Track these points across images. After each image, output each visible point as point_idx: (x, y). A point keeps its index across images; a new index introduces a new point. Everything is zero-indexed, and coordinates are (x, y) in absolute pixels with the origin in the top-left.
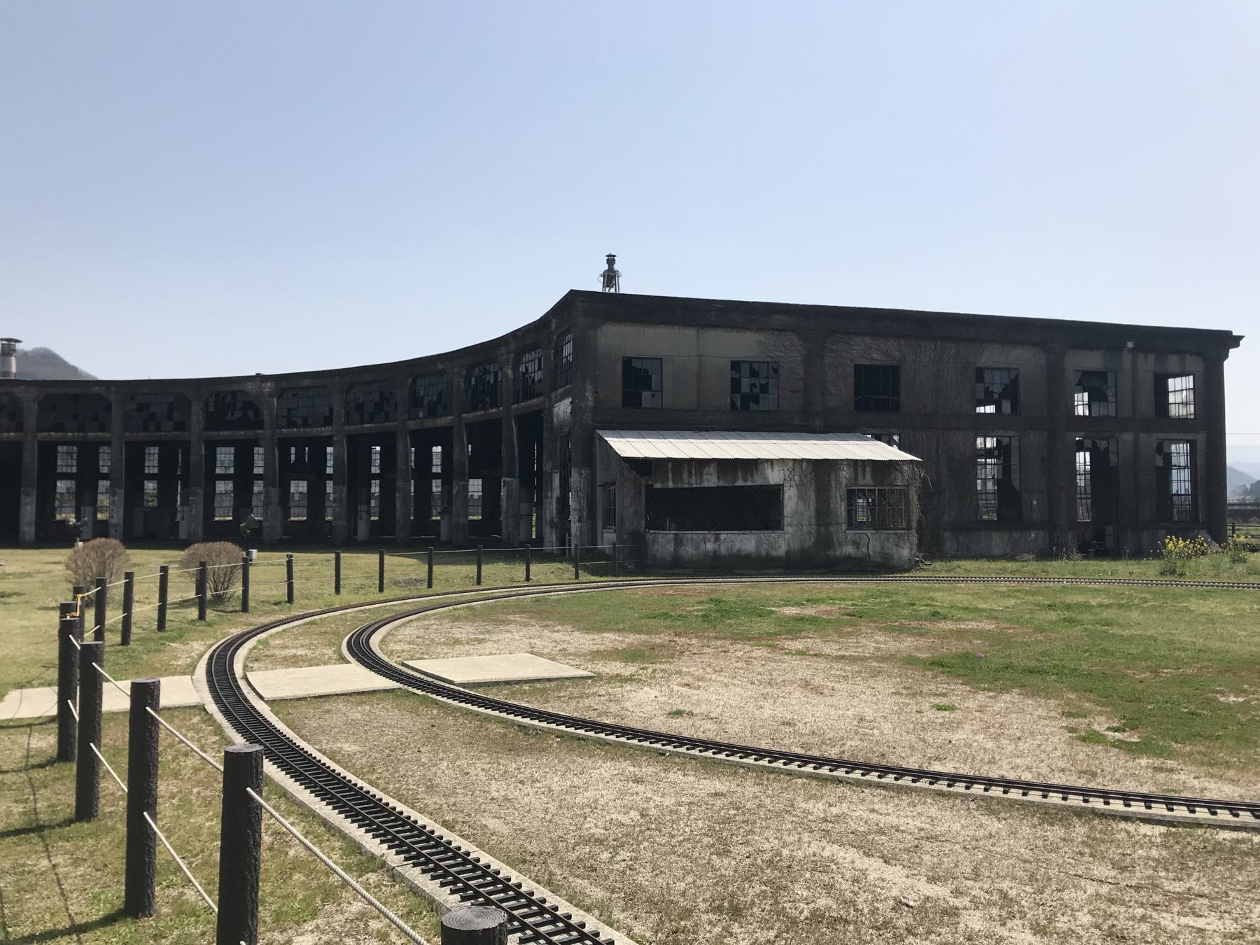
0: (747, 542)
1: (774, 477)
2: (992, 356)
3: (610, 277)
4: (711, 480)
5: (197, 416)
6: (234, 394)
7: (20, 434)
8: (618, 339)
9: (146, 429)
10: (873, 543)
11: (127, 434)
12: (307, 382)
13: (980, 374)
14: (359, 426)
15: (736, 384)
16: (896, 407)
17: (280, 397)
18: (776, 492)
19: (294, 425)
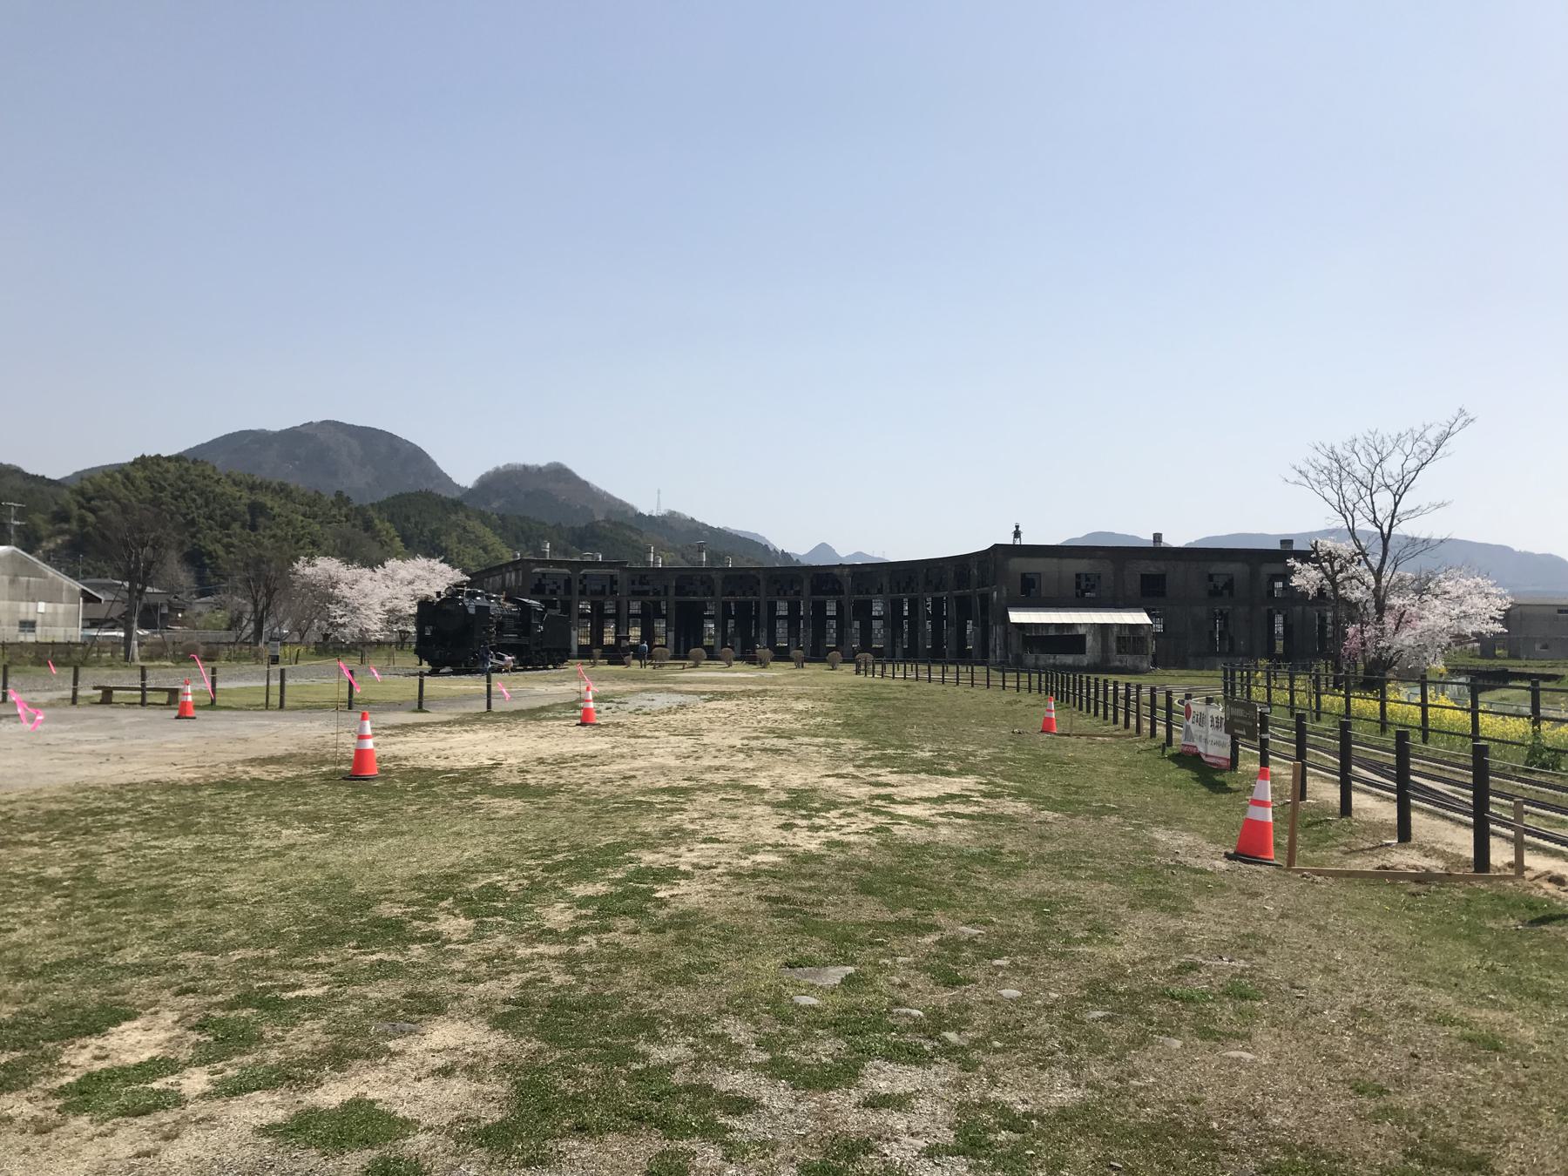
0: (1069, 659)
1: (1081, 631)
2: (1217, 568)
3: (1017, 534)
4: (1052, 633)
5: (807, 585)
8: (1018, 565)
10: (1129, 660)
13: (1211, 577)
15: (1078, 585)
16: (1163, 594)
18: (1083, 637)
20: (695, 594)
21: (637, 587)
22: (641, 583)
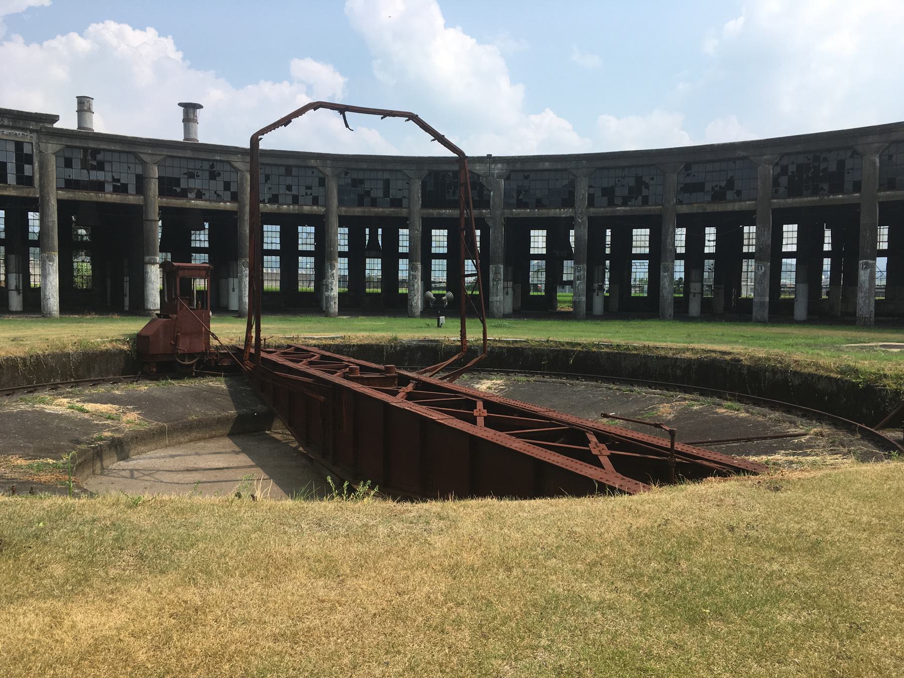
7: (236, 205)
9: (361, 204)
11: (343, 209)
12: (547, 165)
14: (609, 209)
17: (508, 178)
19: (525, 205)
20: (199, 196)
21: (76, 173)
22: (85, 166)
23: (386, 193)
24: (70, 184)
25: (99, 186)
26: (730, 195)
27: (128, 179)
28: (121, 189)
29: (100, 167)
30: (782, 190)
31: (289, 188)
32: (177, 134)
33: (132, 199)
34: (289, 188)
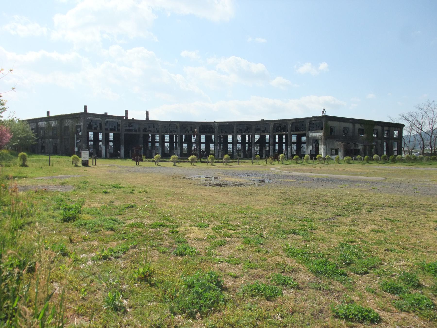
6: (207, 125)
21: (128, 128)
23: (191, 130)
24: (127, 130)
25: (131, 130)
26: (265, 131)
27: (137, 128)
28: (136, 131)
29: (132, 126)
30: (275, 130)
31: (170, 129)
32: (144, 118)
33: (138, 133)
34: (170, 129)
